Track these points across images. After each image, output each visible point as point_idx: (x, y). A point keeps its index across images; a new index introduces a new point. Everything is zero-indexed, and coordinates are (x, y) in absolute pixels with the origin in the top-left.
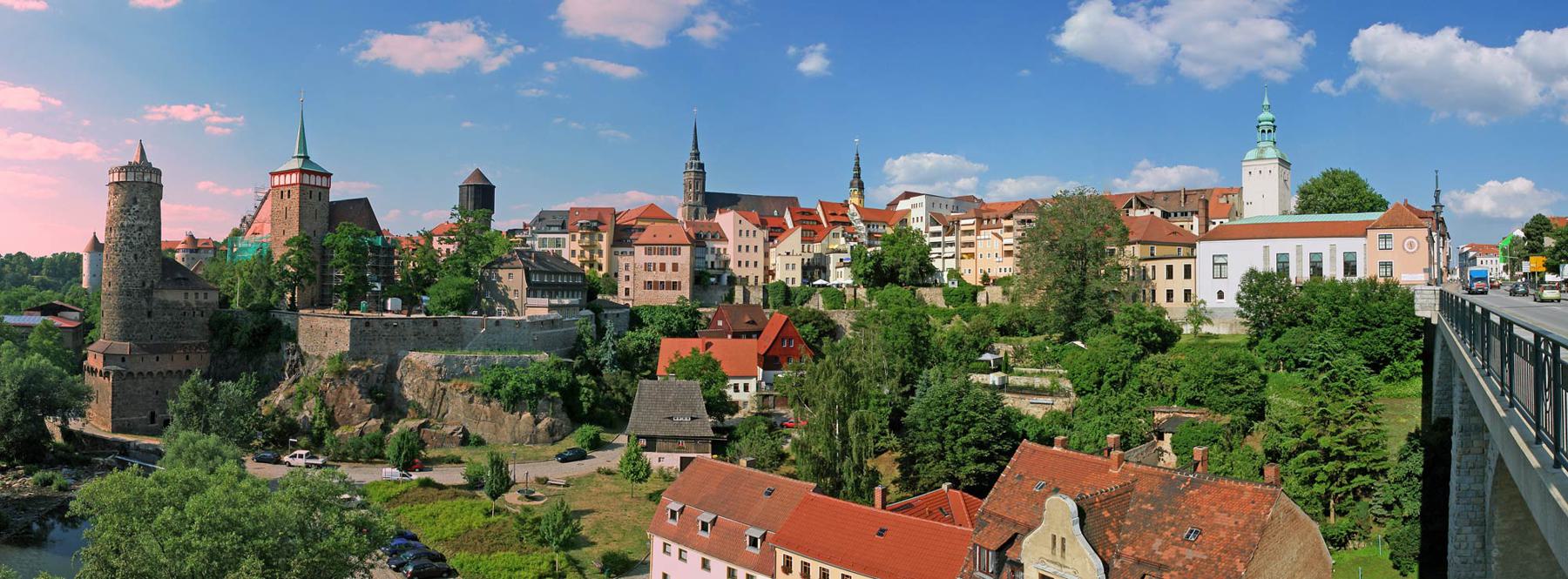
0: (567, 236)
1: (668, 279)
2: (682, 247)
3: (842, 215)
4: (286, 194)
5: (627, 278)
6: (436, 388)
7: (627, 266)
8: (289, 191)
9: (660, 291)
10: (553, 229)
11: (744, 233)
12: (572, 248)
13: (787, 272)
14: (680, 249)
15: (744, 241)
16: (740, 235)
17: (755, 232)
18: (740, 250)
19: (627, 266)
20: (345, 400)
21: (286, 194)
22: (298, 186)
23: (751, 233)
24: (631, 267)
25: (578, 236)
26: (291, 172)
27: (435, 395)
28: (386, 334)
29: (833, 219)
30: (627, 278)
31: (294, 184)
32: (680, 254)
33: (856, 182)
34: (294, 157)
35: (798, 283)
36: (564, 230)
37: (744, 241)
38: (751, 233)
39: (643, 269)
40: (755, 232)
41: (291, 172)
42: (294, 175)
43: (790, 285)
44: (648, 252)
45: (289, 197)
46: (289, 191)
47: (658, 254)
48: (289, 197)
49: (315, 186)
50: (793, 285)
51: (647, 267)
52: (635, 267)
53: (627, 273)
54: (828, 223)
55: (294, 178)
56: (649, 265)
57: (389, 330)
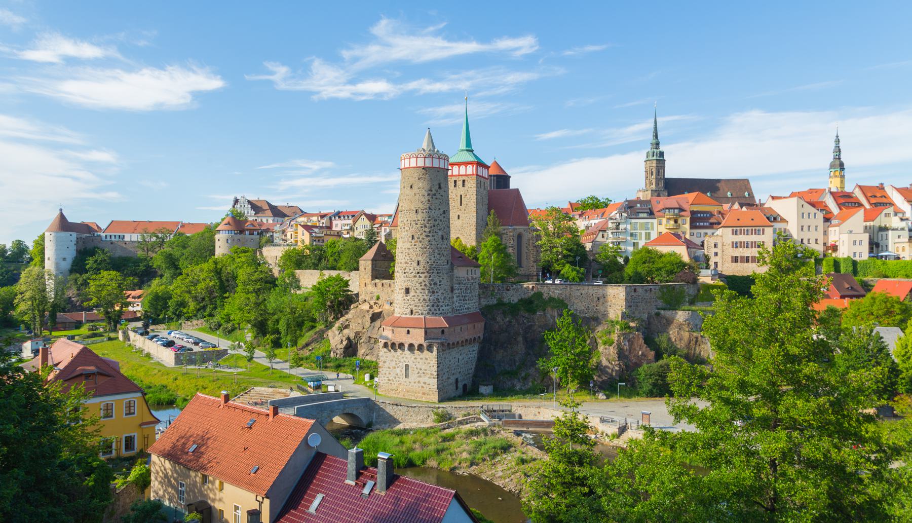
0: (655, 221)
1: (753, 255)
2: (766, 228)
3: (881, 197)
4: (460, 183)
5: (716, 254)
6: (690, 337)
7: (715, 246)
8: (464, 181)
9: (746, 264)
10: (641, 215)
11: (806, 215)
12: (659, 231)
13: (855, 247)
14: (763, 230)
15: (806, 222)
16: (803, 217)
17: (815, 214)
18: (802, 229)
19: (715, 246)
20: (635, 349)
21: (460, 183)
22: (475, 177)
23: (812, 216)
24: (719, 245)
25: (664, 220)
26: (466, 164)
27: (690, 342)
28: (646, 297)
29: (874, 201)
30: (716, 254)
31: (470, 175)
32: (763, 234)
33: (838, 162)
34: (462, 151)
35: (865, 256)
36: (652, 216)
37: (806, 222)
38: (812, 216)
39: (731, 246)
40: (815, 214)
41: (466, 164)
42: (470, 167)
43: (857, 258)
44: (735, 233)
45: (463, 185)
46: (464, 181)
47: (744, 234)
48: (463, 185)
49: (482, 177)
50: (861, 259)
51: (735, 245)
52: (723, 245)
53: (716, 250)
54: (871, 204)
55: (470, 169)
56: (736, 243)
57: (647, 294)
